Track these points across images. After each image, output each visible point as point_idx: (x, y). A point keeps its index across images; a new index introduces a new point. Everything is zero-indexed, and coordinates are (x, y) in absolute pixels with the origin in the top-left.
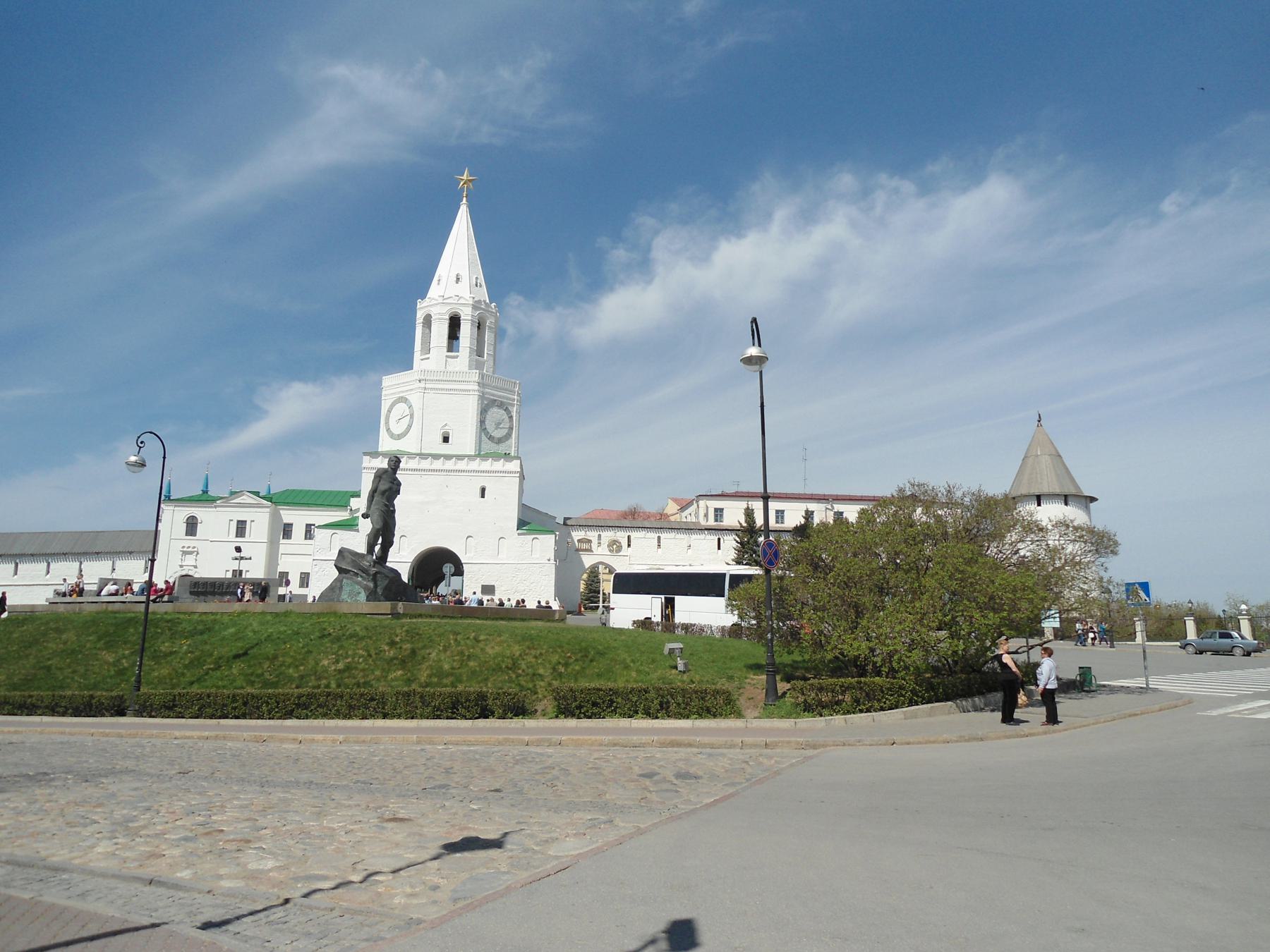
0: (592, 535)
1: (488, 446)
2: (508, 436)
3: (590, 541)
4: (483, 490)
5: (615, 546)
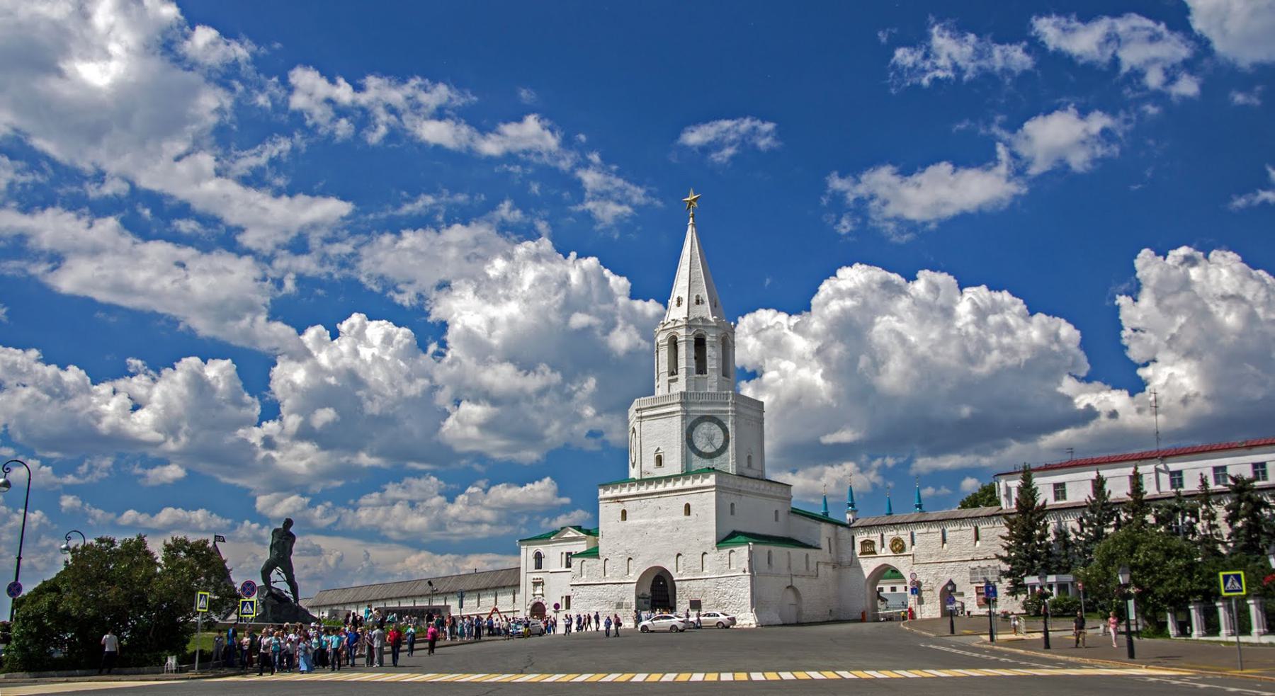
0: (875, 536)
1: (698, 463)
2: (724, 448)
3: (872, 543)
4: (688, 507)
5: (898, 546)
